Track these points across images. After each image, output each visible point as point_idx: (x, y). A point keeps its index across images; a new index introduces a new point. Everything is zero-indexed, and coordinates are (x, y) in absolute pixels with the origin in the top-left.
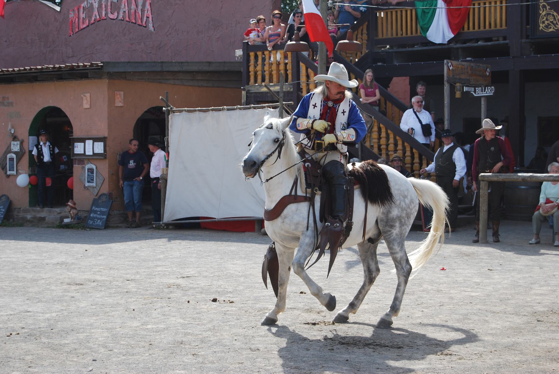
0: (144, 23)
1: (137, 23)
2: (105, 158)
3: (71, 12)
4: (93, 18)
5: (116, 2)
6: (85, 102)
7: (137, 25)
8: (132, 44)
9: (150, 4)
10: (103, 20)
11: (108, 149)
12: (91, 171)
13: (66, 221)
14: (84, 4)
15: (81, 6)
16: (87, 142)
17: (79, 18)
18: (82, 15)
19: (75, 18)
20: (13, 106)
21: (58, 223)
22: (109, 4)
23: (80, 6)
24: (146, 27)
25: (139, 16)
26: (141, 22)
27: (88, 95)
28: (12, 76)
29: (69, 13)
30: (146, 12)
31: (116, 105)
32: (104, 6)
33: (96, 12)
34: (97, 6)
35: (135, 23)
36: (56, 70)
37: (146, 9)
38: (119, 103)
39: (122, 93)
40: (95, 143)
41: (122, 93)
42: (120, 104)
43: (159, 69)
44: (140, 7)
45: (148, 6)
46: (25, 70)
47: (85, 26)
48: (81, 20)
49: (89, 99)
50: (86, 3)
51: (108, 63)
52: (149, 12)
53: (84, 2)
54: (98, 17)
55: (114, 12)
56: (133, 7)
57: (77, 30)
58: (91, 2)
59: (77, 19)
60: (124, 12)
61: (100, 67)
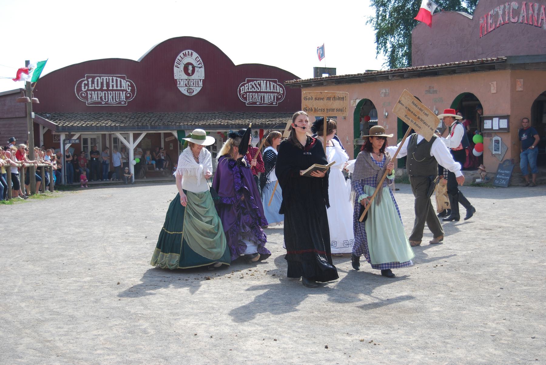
0: (539, 24)
1: (534, 25)
2: (509, 132)
3: (481, 19)
4: (498, 23)
5: (516, 8)
6: (492, 88)
7: (533, 26)
8: (529, 42)
9: (544, 9)
10: (506, 24)
11: (510, 124)
12: (497, 142)
13: (478, 180)
14: (491, 12)
15: (489, 14)
16: (494, 119)
17: (487, 23)
18: (490, 21)
19: (484, 23)
20: (437, 93)
21: (471, 182)
22: (511, 11)
23: (488, 14)
24: (541, 27)
25: (535, 19)
26: (537, 23)
27: (495, 83)
28: (436, 70)
29: (479, 20)
30: (541, 15)
31: (517, 90)
32: (507, 13)
33: (500, 18)
34: (501, 13)
35: (532, 25)
36: (470, 64)
37: (541, 13)
38: (519, 88)
39: (522, 80)
40: (501, 120)
41: (522, 80)
42: (521, 89)
44: (536, 12)
45: (542, 11)
46: (446, 65)
47: (492, 29)
48: (489, 25)
49: (496, 86)
50: (493, 11)
51: (510, 57)
52: (544, 16)
53: (491, 10)
54: (502, 22)
55: (515, 17)
56: (531, 12)
57: (486, 33)
58: (496, 10)
59: (486, 25)
60: (523, 16)
61: (504, 61)
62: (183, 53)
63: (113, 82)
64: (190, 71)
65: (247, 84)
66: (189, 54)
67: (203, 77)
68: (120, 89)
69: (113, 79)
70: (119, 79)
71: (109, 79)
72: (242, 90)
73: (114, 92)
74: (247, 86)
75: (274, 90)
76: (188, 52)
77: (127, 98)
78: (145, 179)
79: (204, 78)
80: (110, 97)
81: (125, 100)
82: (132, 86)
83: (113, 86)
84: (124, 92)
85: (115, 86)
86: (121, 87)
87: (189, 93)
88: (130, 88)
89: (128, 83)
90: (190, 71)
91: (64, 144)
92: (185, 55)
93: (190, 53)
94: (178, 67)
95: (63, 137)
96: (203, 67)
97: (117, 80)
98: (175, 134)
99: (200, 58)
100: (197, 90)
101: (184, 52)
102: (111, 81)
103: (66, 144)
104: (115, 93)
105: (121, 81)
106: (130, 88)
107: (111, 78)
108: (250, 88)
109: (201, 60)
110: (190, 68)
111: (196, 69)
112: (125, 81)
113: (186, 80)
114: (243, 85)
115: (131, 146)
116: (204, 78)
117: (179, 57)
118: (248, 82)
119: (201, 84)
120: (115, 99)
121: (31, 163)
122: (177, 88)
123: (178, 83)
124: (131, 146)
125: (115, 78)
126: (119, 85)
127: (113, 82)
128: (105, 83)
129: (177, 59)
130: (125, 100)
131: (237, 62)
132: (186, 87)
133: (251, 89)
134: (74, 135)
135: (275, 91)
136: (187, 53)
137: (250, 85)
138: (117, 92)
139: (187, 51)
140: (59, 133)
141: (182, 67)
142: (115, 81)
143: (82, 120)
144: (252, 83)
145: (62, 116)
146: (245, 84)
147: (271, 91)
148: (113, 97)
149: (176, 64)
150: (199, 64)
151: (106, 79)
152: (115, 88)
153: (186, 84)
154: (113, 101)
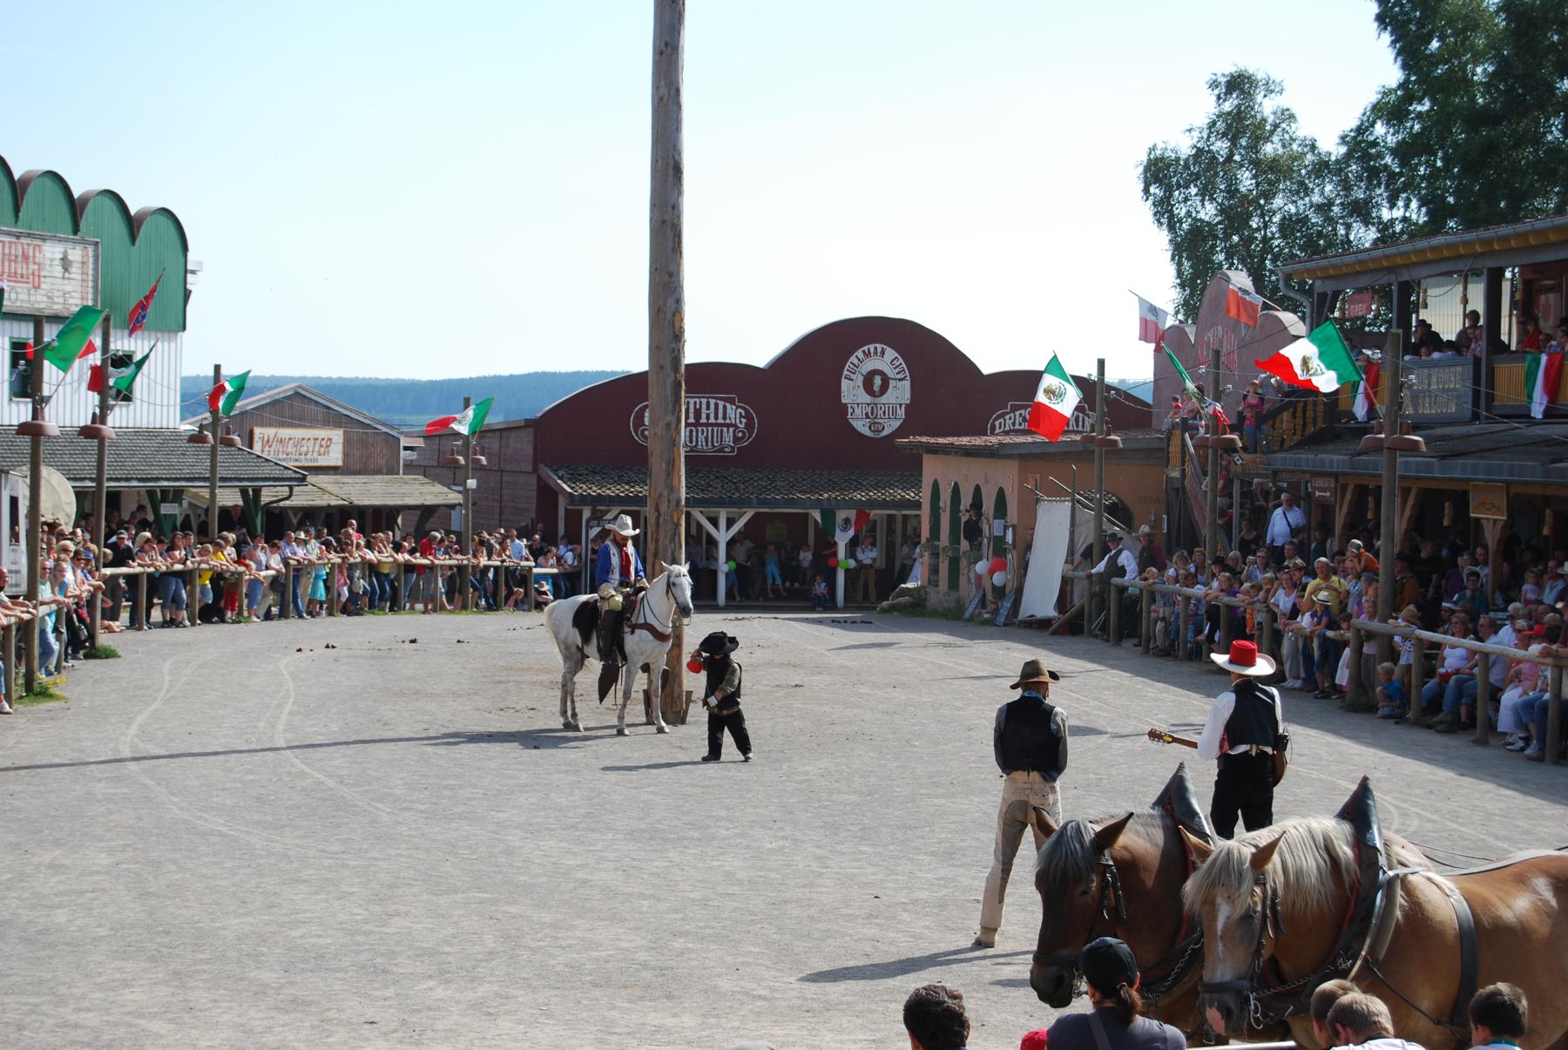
11: (1017, 538)
43: (1081, 449)
62: (864, 352)
63: (708, 408)
64: (876, 388)
65: (1012, 415)
66: (876, 353)
67: (906, 397)
68: (723, 422)
69: (708, 404)
70: (721, 404)
71: (701, 403)
72: (998, 426)
73: (710, 429)
74: (1010, 418)
75: (1077, 426)
76: (876, 348)
77: (736, 439)
78: (761, 603)
79: (908, 402)
80: (701, 438)
81: (731, 444)
82: (748, 416)
83: (708, 417)
84: (731, 429)
85: (712, 416)
86: (724, 418)
87: (874, 431)
88: (744, 421)
89: (739, 410)
90: (876, 388)
91: (589, 527)
92: (867, 354)
93: (879, 350)
94: (850, 379)
95: (586, 514)
96: (908, 378)
97: (716, 405)
98: (816, 515)
99: (901, 360)
100: (891, 426)
101: (865, 348)
102: (704, 406)
103: (592, 528)
104: (713, 431)
105: (725, 407)
106: (744, 421)
107: (704, 401)
108: (1017, 422)
109: (904, 365)
110: (878, 381)
111: (892, 383)
112: (734, 407)
113: (868, 405)
114: (1002, 416)
115: (723, 536)
116: (908, 402)
117: (853, 359)
118: (1014, 409)
119: (901, 413)
120: (712, 442)
121: (462, 560)
122: (847, 420)
123: (850, 410)
124: (723, 536)
125: (712, 402)
126: (720, 415)
127: (708, 408)
128: (692, 410)
129: (849, 363)
130: (731, 444)
131: (987, 368)
132: (868, 420)
133: (1020, 424)
134: (607, 512)
135: (1080, 429)
136: (872, 350)
137: (1017, 417)
138: (715, 429)
139: (872, 347)
140: (579, 508)
141: (859, 380)
142: (712, 406)
143: (627, 484)
144: (1023, 412)
145: (596, 473)
146: (1007, 413)
147: (1071, 428)
148: (706, 438)
149: (845, 372)
150: (899, 373)
151: (695, 403)
152: (712, 420)
153: (867, 414)
154: (707, 445)
